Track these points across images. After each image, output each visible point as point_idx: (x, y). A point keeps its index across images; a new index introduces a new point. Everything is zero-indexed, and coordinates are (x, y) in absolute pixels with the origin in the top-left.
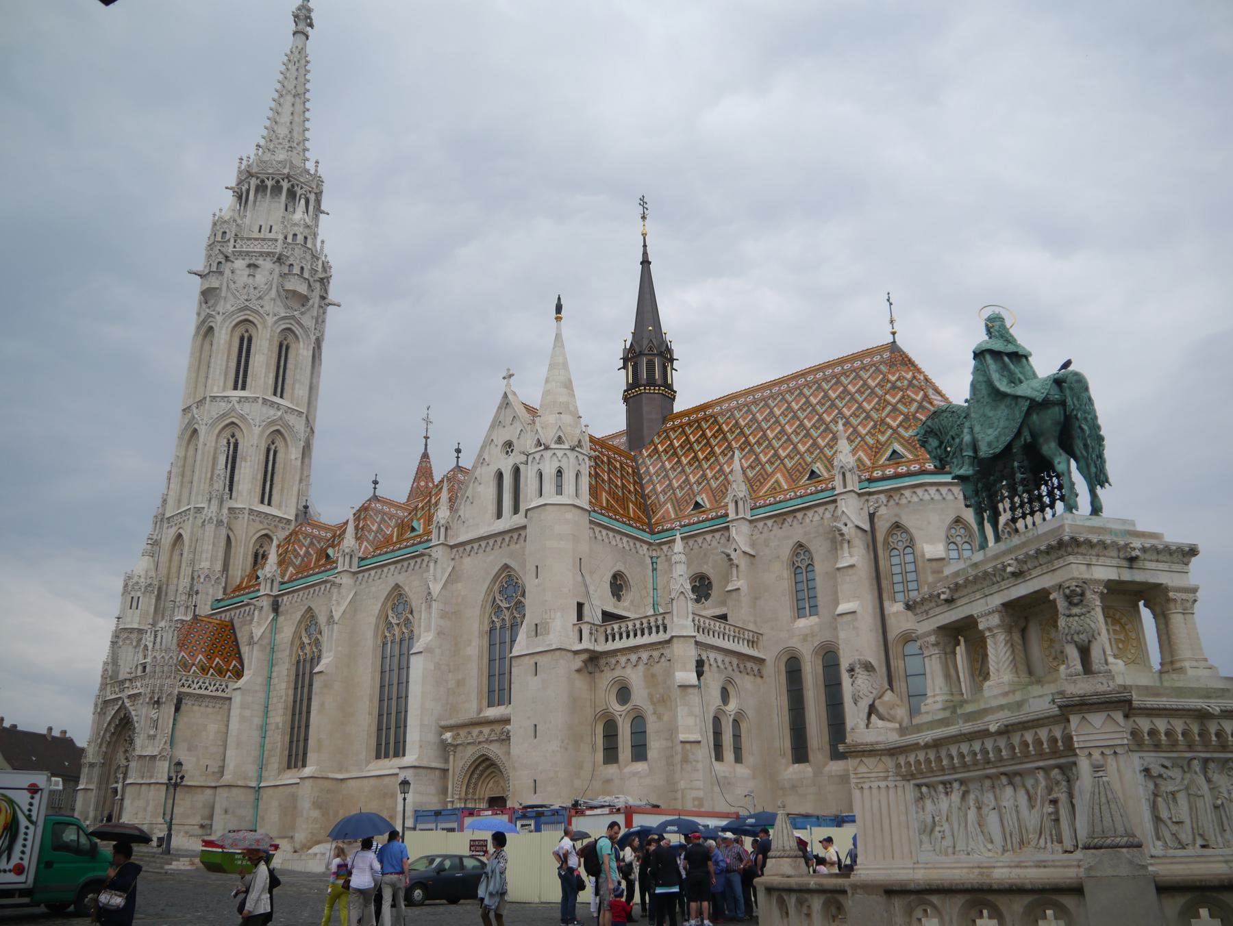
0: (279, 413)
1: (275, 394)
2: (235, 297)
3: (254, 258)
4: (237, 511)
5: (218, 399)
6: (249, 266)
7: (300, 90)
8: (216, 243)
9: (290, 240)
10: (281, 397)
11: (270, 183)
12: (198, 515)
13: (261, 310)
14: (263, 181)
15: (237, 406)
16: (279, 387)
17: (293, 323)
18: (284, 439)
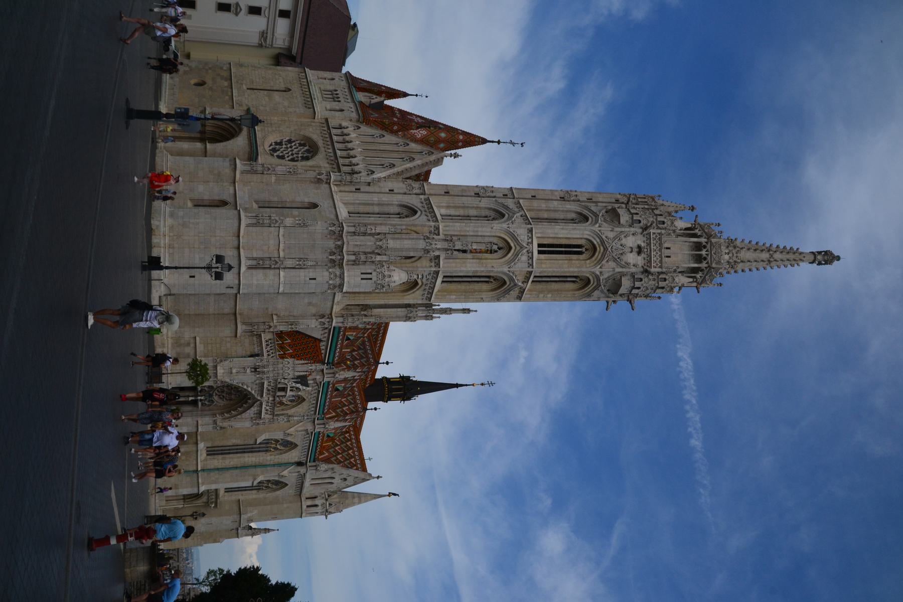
0: (520, 284)
1: (535, 277)
2: (615, 238)
3: (646, 250)
4: (437, 261)
5: (530, 235)
6: (639, 247)
7: (773, 264)
8: (655, 217)
9: (662, 276)
10: (533, 281)
11: (704, 252)
12: (432, 229)
13: (604, 262)
14: (705, 247)
15: (525, 251)
16: (541, 279)
17: (594, 286)
18: (499, 288)
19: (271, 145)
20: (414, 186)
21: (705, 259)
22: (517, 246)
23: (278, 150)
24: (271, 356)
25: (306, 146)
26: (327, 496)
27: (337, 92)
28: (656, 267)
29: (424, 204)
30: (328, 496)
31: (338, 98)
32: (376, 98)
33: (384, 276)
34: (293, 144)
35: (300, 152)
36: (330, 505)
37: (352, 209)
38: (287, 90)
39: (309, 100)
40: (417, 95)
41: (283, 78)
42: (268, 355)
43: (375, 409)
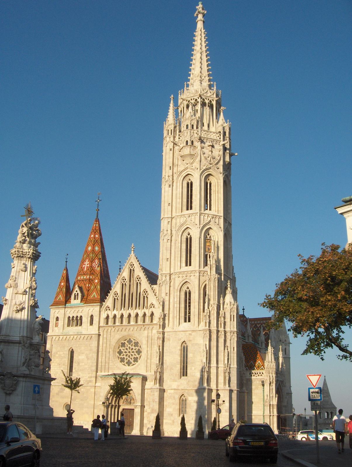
19: (124, 365)
20: (163, 280)
21: (210, 101)
22: (209, 224)
23: (129, 360)
24: (262, 374)
25: (125, 343)
26: (280, 342)
27: (71, 317)
28: (220, 138)
29: (181, 276)
30: (280, 341)
31: (77, 317)
32: (77, 291)
33: (232, 308)
34: (122, 350)
35: (131, 347)
36: (285, 341)
37: (182, 320)
38: (71, 350)
39: (83, 336)
40: (67, 262)
41: (59, 351)
42: (261, 375)
43: (243, 309)
